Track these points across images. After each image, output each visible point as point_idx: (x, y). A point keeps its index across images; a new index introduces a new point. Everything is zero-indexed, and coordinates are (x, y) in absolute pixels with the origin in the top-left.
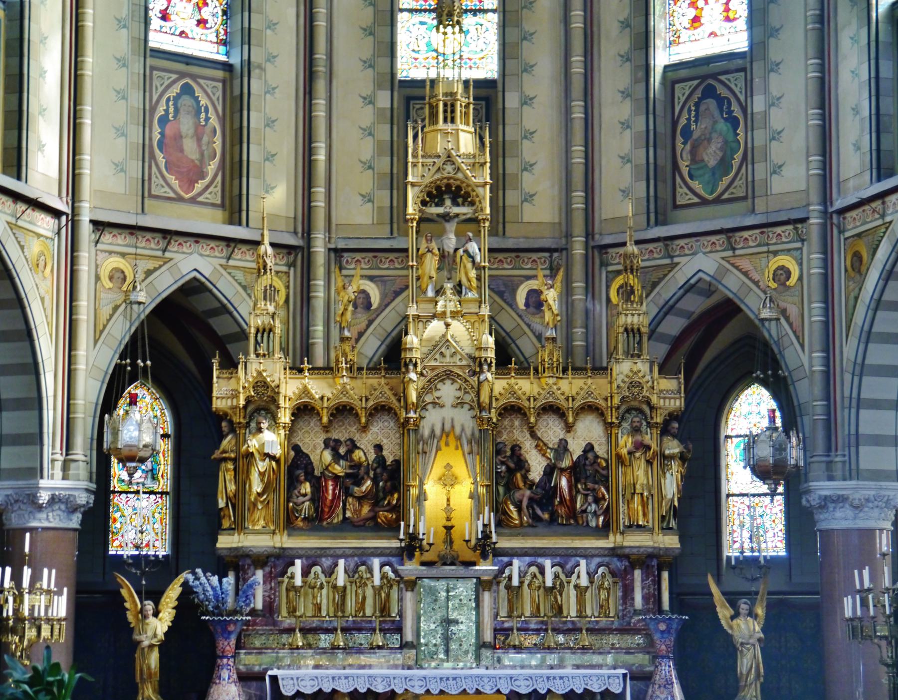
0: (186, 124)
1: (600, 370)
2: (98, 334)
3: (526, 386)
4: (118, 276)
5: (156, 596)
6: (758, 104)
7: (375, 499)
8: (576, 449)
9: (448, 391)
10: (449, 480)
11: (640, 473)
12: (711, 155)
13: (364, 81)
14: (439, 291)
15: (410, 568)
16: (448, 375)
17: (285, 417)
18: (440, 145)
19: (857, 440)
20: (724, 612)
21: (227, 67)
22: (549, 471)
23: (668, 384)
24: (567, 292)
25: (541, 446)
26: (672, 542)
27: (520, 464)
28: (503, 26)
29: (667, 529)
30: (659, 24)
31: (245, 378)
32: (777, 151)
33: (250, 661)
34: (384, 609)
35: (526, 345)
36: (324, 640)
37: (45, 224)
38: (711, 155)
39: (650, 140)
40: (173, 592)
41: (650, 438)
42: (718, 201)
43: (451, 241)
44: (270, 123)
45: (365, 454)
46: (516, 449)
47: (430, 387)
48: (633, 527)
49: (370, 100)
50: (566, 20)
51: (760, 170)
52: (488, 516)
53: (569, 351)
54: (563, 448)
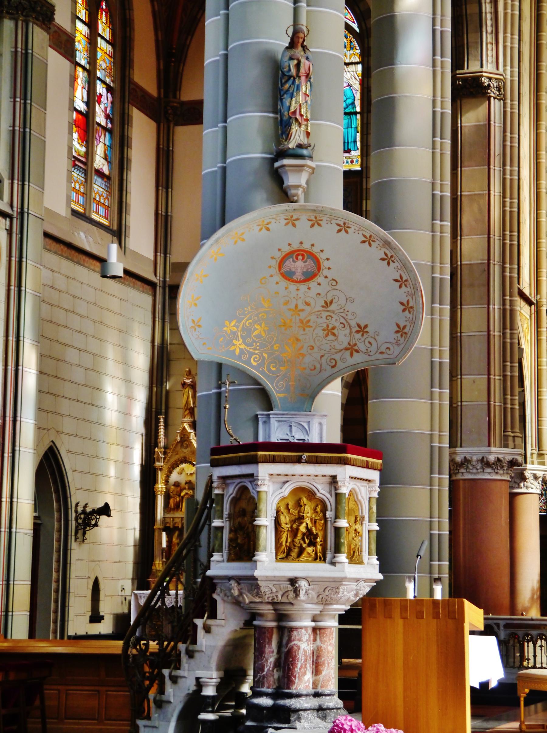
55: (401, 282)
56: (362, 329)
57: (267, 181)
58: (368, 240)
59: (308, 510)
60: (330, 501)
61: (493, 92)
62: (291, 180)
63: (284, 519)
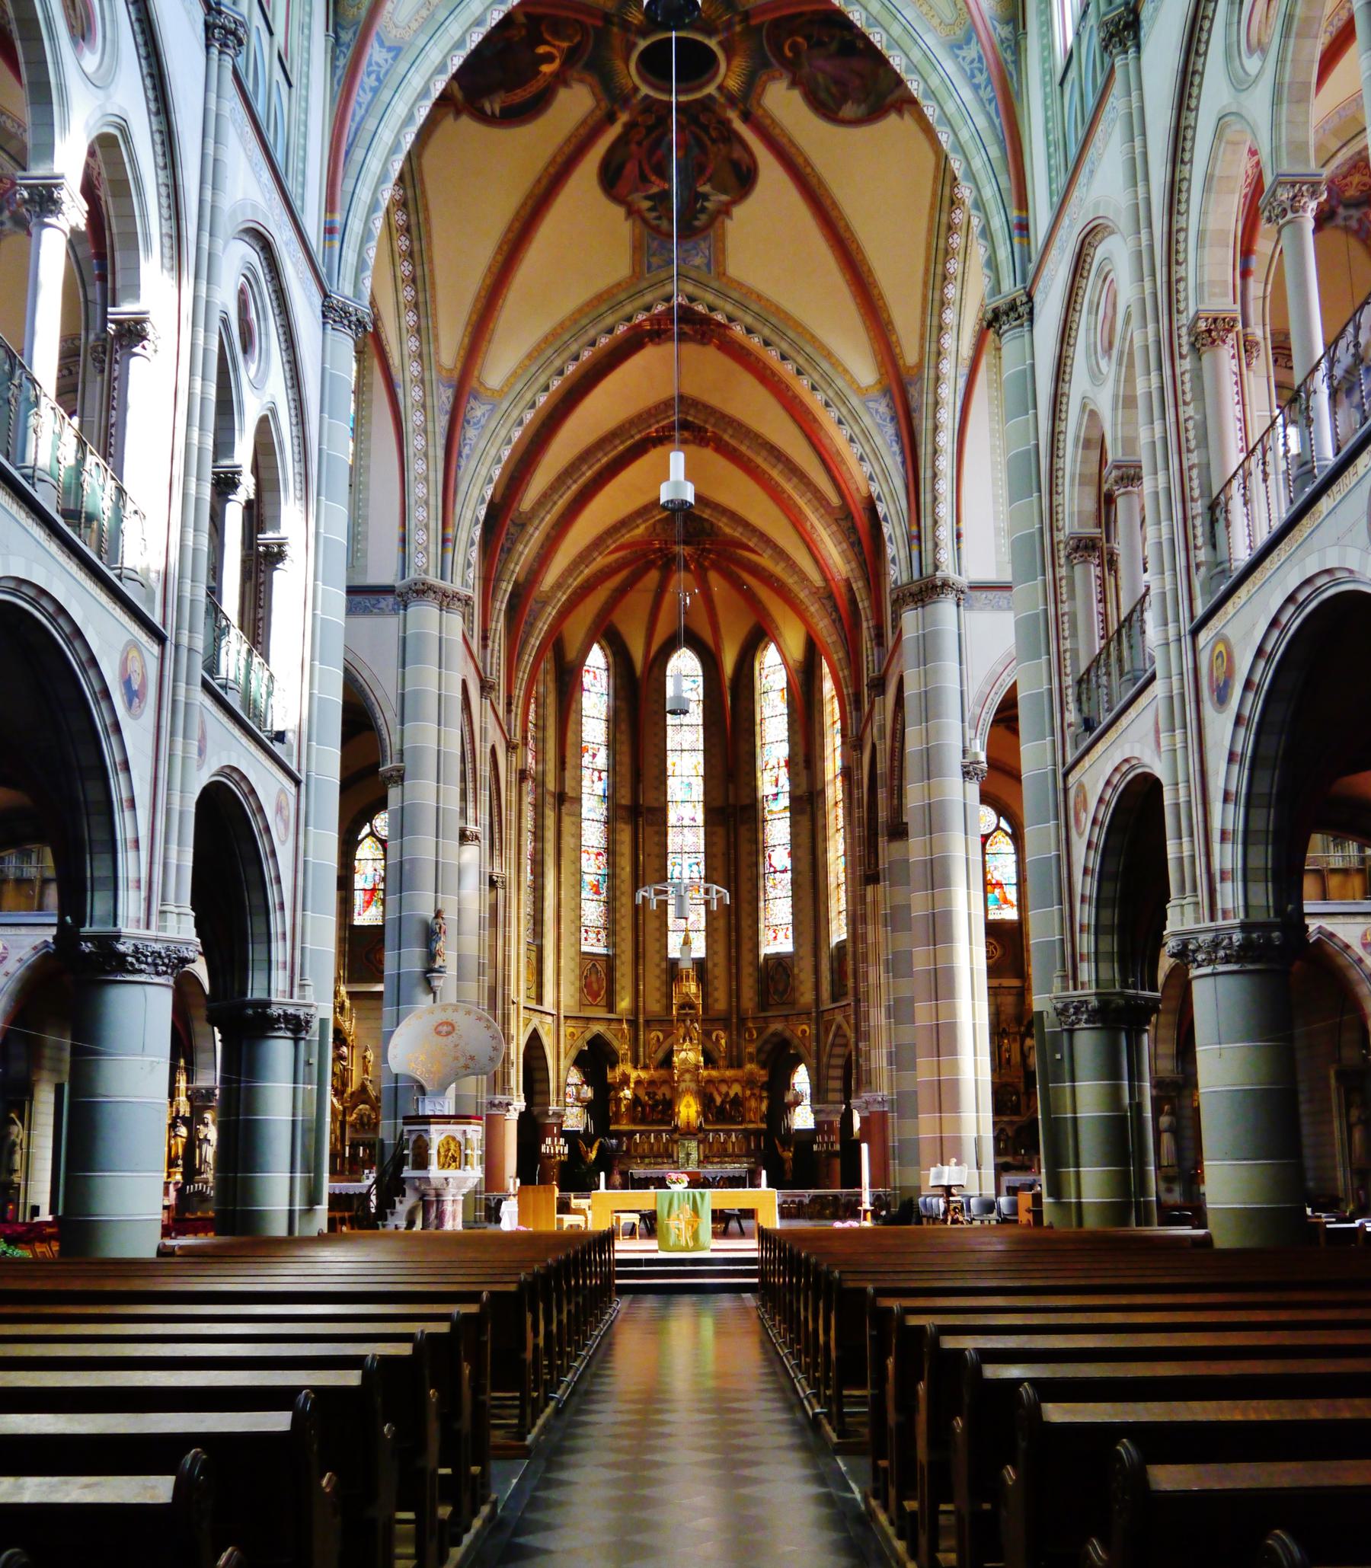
0: (594, 978)
1: (740, 1066)
2: (566, 1055)
3: (714, 1073)
4: (572, 1034)
5: (590, 1145)
6: (796, 970)
7: (663, 1112)
8: (732, 1094)
9: (687, 1076)
10: (688, 1106)
11: (753, 1103)
12: (781, 988)
13: (657, 959)
14: (684, 1040)
15: (676, 1136)
16: (688, 1071)
17: (632, 1085)
18: (684, 990)
19: (827, 1091)
20: (780, 1150)
21: (607, 955)
22: (723, 1102)
23: (762, 1072)
24: (730, 1037)
25: (720, 1094)
26: (764, 1126)
27: (712, 1099)
28: (707, 937)
29: (762, 1121)
30: (762, 938)
31: (618, 1071)
32: (803, 988)
33: (622, 1167)
34: (667, 1150)
35: (716, 1055)
36: (647, 1160)
37: (549, 1019)
38: (781, 988)
39: (759, 981)
40: (596, 1145)
41: (757, 1091)
42: (784, 1003)
43: (688, 1022)
44: (623, 975)
45: (659, 1097)
46: (711, 1095)
47: (681, 1075)
48: (751, 1122)
49: (658, 965)
50: (729, 936)
51: (797, 995)
52: (701, 1119)
53: (731, 1059)
54: (727, 1094)
55: (493, 1037)
56: (472, 1058)
57: (424, 984)
58: (479, 1019)
59: (452, 1146)
60: (463, 1141)
61: (499, 885)
62: (436, 983)
63: (442, 1151)
